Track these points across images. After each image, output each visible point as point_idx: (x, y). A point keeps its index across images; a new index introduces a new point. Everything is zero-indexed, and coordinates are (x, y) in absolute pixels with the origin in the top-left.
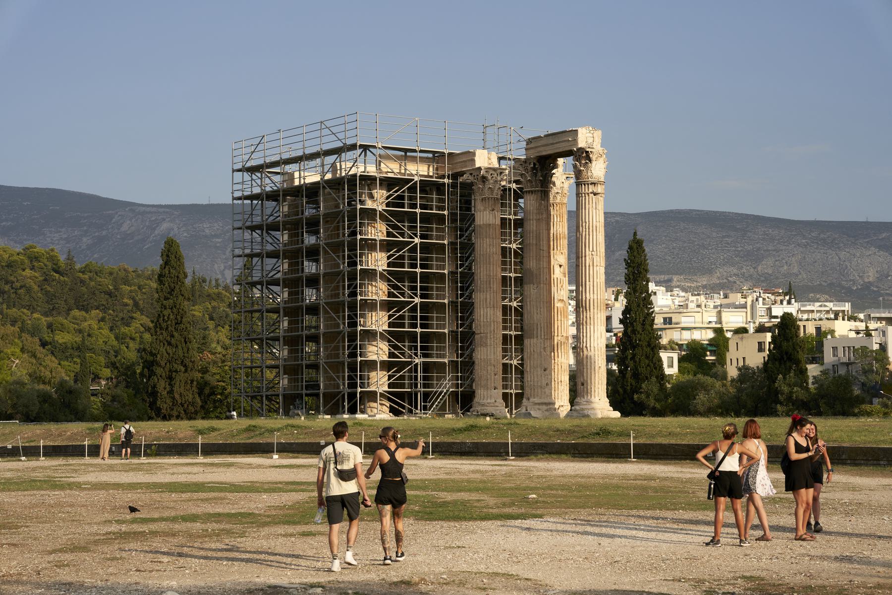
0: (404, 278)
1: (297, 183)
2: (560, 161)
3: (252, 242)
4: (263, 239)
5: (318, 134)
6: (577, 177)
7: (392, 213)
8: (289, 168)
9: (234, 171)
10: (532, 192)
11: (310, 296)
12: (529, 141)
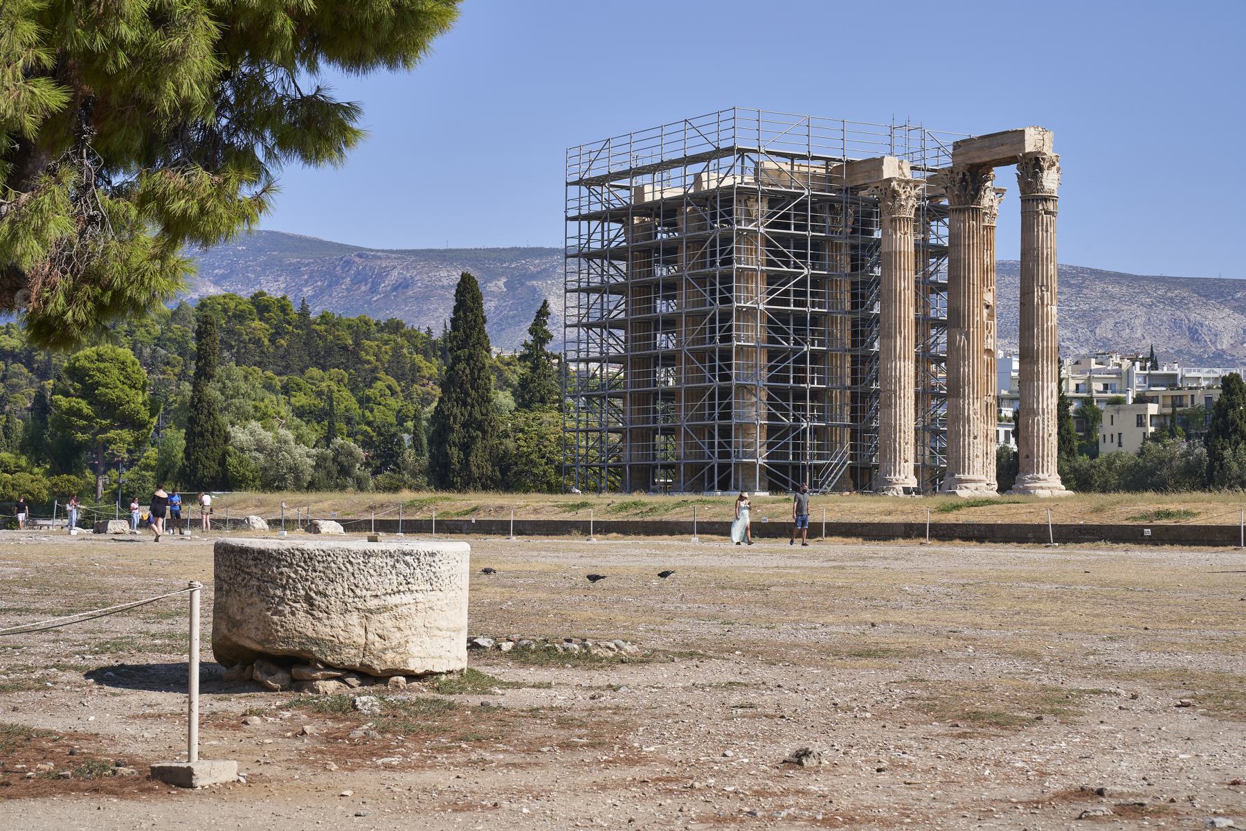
0: (789, 320)
1: (648, 198)
2: (996, 171)
3: (589, 274)
4: (603, 270)
5: (658, 141)
6: (1023, 191)
7: (779, 238)
8: (638, 181)
9: (567, 184)
10: (960, 209)
11: (664, 341)
12: (957, 145)
